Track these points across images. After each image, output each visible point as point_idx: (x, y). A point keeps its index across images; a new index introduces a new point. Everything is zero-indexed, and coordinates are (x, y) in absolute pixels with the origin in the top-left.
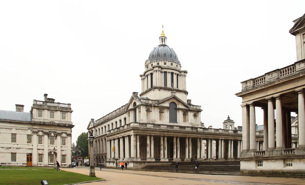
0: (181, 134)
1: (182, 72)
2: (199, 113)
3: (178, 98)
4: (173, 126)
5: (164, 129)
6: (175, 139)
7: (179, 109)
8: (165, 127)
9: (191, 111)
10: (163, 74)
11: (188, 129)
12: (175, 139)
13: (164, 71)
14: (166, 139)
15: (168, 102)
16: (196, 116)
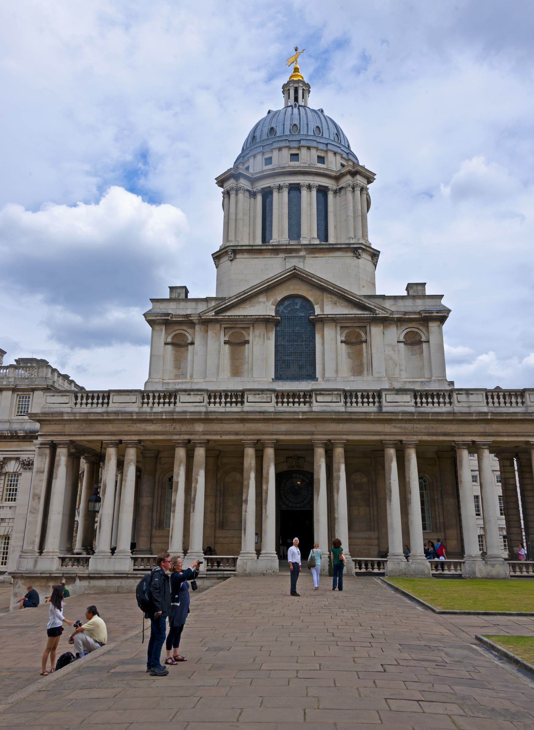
0: (283, 427)
1: (342, 175)
2: (433, 326)
3: (314, 276)
4: (243, 392)
5: (197, 409)
6: (250, 452)
7: (323, 320)
8: (198, 398)
9: (385, 321)
10: (259, 198)
11: (320, 398)
12: (250, 452)
13: (259, 188)
14: (200, 453)
15: (272, 301)
16: (420, 342)
